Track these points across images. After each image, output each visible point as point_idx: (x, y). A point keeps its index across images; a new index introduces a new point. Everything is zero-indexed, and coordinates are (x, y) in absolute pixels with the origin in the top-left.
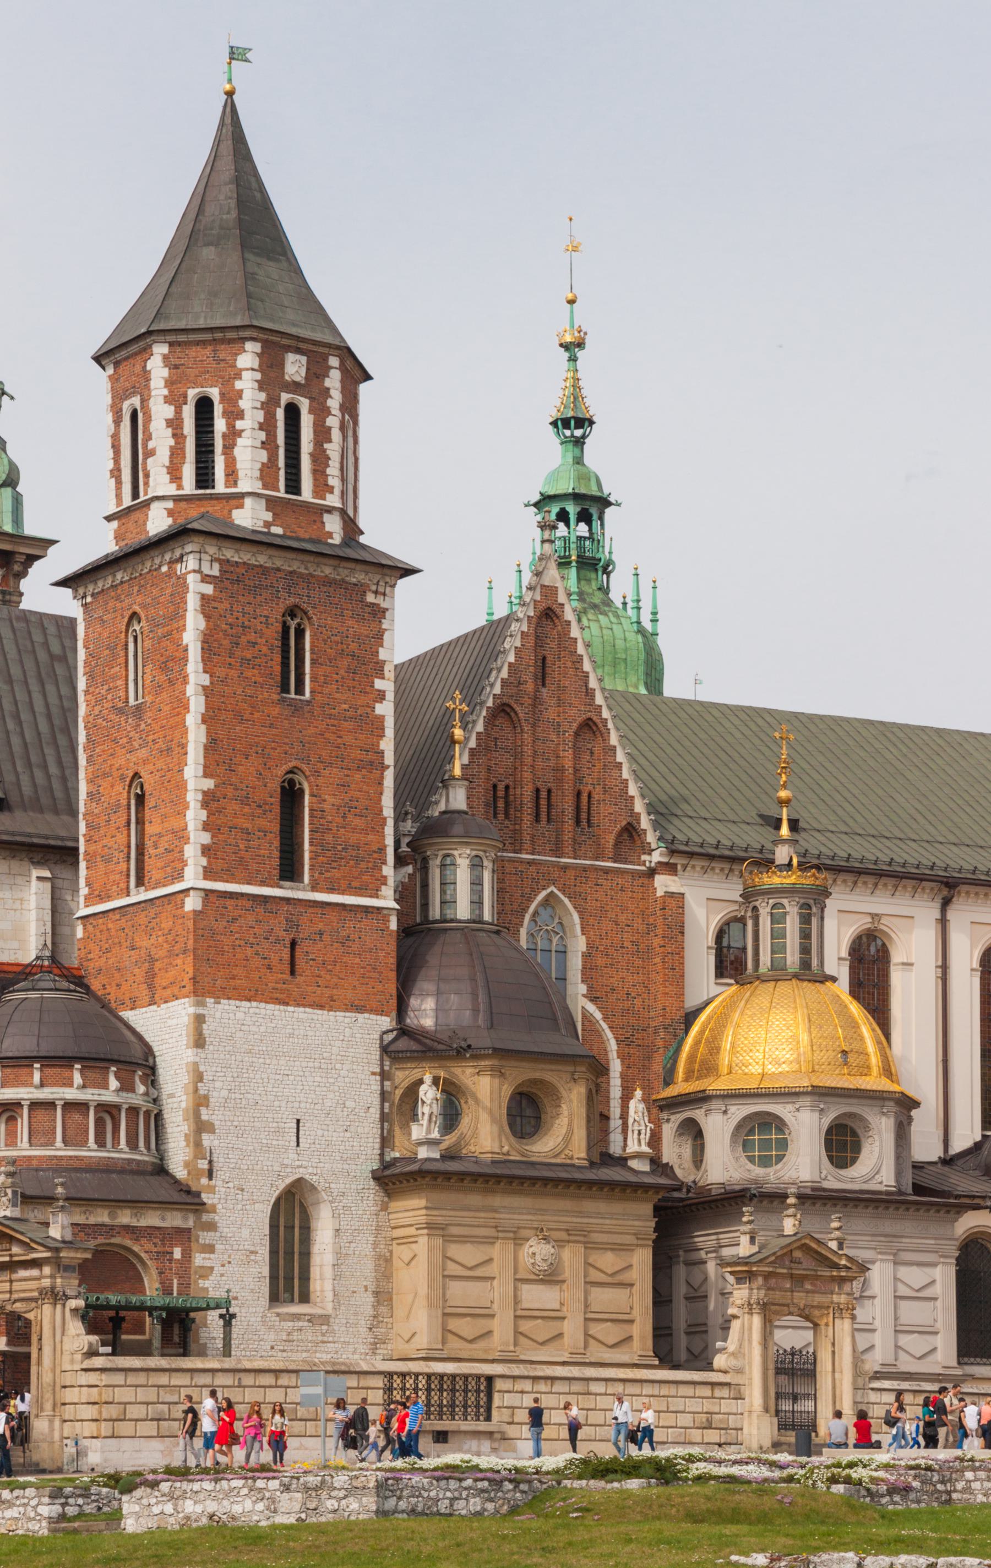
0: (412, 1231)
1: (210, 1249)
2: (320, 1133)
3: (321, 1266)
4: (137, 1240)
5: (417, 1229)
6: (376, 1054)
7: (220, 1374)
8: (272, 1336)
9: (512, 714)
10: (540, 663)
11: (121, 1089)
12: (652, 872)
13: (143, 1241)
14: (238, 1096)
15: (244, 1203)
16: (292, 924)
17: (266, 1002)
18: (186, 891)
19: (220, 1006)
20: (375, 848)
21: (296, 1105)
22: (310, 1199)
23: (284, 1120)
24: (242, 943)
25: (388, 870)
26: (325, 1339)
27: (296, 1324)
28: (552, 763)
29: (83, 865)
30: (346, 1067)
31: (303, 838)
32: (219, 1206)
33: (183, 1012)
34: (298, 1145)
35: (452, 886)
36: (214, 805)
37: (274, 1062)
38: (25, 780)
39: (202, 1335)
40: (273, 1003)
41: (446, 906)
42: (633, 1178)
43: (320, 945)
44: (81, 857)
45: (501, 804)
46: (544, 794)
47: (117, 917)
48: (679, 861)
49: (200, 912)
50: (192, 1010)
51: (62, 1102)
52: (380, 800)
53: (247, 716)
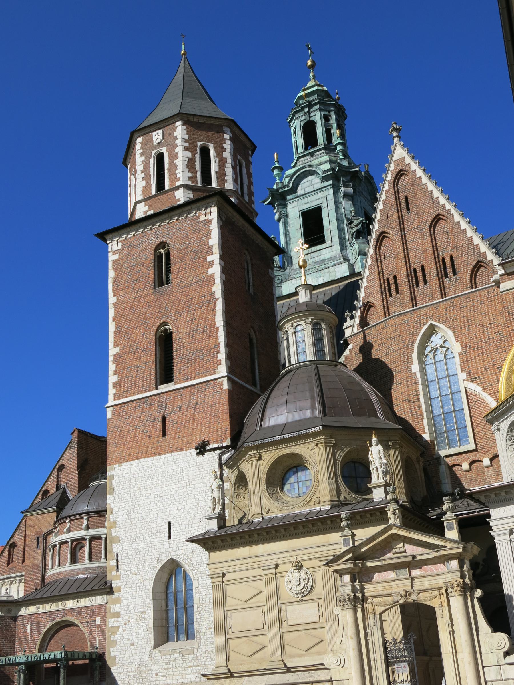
1: (117, 615)
2: (183, 527)
8: (155, 667)
9: (389, 236)
10: (403, 201)
12: (498, 284)
14: (132, 517)
15: (137, 582)
17: (148, 457)
19: (122, 467)
20: (212, 347)
23: (160, 525)
25: (222, 356)
26: (192, 664)
27: (172, 656)
30: (198, 482)
32: (123, 587)
34: (170, 538)
36: (119, 360)
37: (154, 490)
40: (152, 456)
43: (180, 414)
45: (393, 288)
46: (419, 270)
49: (111, 419)
52: (215, 319)
53: (136, 307)
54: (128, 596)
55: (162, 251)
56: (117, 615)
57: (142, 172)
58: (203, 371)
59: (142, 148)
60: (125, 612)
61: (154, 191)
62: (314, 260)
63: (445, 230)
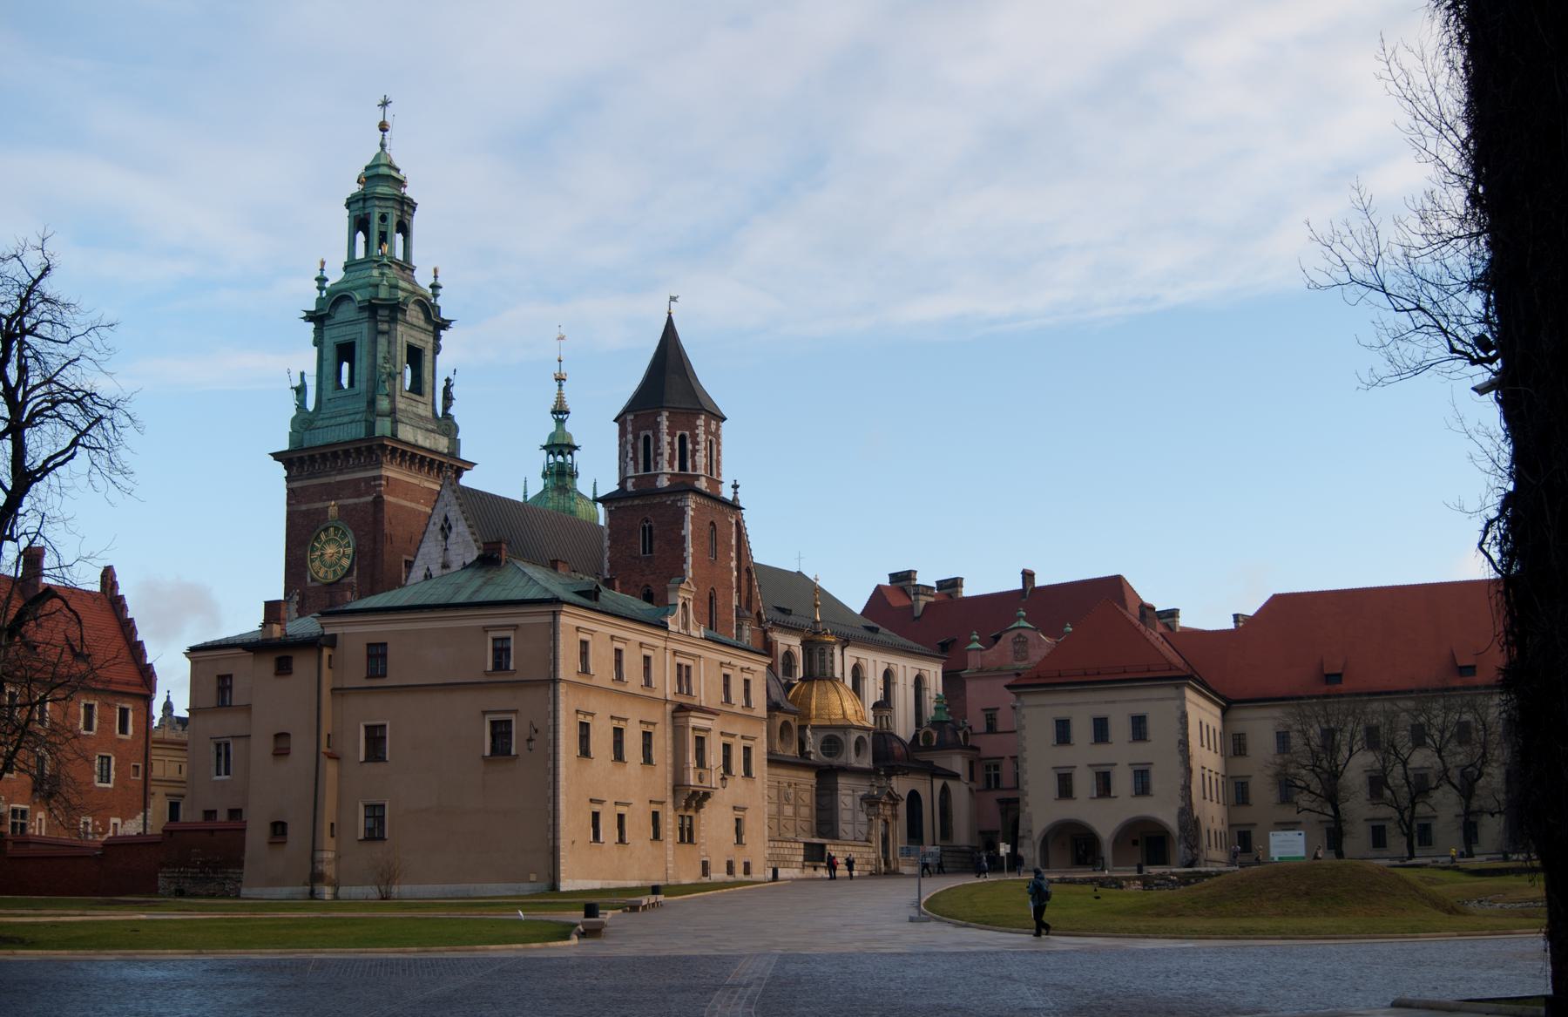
12: (765, 632)
25: (734, 631)
42: (811, 762)
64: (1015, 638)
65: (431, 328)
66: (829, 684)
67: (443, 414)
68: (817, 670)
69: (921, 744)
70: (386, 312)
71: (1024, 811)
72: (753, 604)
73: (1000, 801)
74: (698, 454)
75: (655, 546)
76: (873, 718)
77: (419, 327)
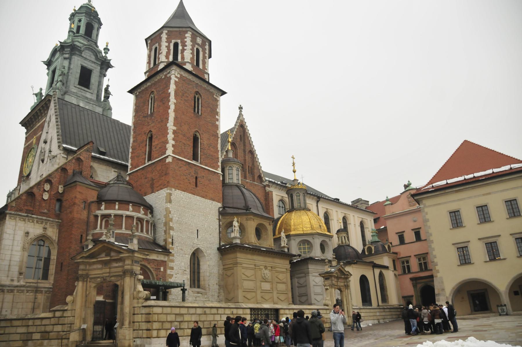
0: (231, 266)
1: (172, 268)
2: (204, 235)
3: (204, 277)
4: (149, 263)
5: (233, 265)
6: (217, 214)
7: (198, 309)
11: (144, 214)
12: (265, 186)
13: (151, 264)
14: (181, 220)
16: (196, 173)
18: (167, 157)
19: (176, 192)
21: (197, 225)
22: (200, 255)
24: (183, 174)
25: (220, 164)
26: (206, 300)
28: (243, 158)
29: (130, 161)
30: (210, 216)
31: (198, 151)
32: (175, 255)
33: (165, 192)
34: (198, 238)
35: (231, 175)
38: (112, 151)
39: (169, 297)
41: (229, 180)
44: (130, 158)
47: (141, 171)
48: (270, 184)
49: (171, 163)
50: (168, 191)
51: (125, 215)
52: (217, 145)
54: (178, 260)
55: (197, 96)
56: (172, 268)
57: (191, 50)
58: (212, 165)
59: (191, 38)
60: (176, 268)
61: (195, 65)
62: (81, 93)
63: (251, 156)
64: (407, 196)
65: (100, 63)
66: (303, 211)
67: (104, 101)
68: (296, 205)
69: (367, 253)
70: (69, 50)
71: (436, 277)
72: (255, 171)
73: (412, 279)
74: (185, 51)
75: (155, 106)
76: (337, 239)
77: (90, 60)
